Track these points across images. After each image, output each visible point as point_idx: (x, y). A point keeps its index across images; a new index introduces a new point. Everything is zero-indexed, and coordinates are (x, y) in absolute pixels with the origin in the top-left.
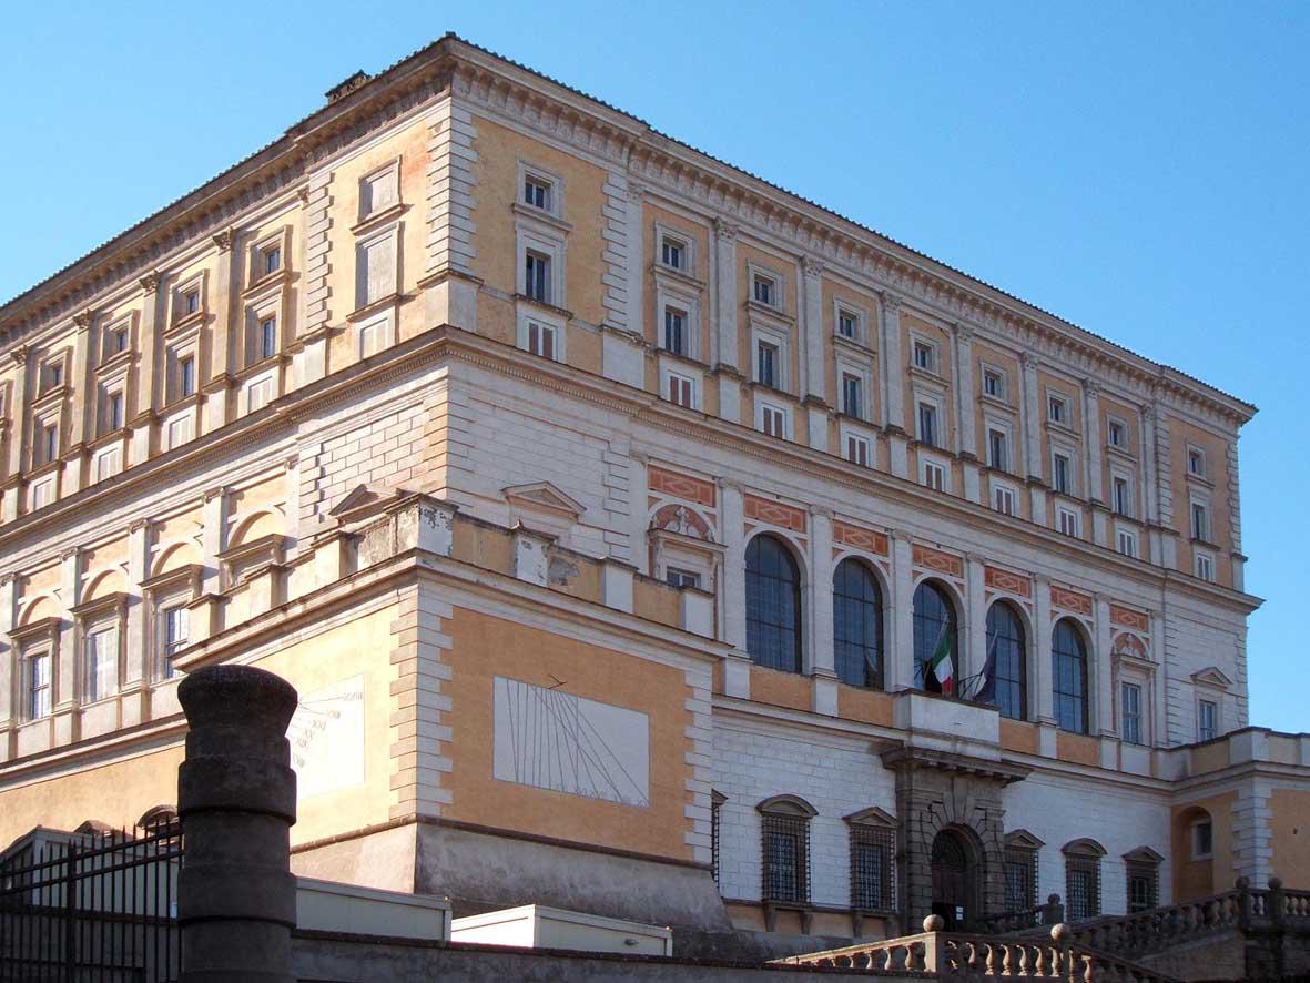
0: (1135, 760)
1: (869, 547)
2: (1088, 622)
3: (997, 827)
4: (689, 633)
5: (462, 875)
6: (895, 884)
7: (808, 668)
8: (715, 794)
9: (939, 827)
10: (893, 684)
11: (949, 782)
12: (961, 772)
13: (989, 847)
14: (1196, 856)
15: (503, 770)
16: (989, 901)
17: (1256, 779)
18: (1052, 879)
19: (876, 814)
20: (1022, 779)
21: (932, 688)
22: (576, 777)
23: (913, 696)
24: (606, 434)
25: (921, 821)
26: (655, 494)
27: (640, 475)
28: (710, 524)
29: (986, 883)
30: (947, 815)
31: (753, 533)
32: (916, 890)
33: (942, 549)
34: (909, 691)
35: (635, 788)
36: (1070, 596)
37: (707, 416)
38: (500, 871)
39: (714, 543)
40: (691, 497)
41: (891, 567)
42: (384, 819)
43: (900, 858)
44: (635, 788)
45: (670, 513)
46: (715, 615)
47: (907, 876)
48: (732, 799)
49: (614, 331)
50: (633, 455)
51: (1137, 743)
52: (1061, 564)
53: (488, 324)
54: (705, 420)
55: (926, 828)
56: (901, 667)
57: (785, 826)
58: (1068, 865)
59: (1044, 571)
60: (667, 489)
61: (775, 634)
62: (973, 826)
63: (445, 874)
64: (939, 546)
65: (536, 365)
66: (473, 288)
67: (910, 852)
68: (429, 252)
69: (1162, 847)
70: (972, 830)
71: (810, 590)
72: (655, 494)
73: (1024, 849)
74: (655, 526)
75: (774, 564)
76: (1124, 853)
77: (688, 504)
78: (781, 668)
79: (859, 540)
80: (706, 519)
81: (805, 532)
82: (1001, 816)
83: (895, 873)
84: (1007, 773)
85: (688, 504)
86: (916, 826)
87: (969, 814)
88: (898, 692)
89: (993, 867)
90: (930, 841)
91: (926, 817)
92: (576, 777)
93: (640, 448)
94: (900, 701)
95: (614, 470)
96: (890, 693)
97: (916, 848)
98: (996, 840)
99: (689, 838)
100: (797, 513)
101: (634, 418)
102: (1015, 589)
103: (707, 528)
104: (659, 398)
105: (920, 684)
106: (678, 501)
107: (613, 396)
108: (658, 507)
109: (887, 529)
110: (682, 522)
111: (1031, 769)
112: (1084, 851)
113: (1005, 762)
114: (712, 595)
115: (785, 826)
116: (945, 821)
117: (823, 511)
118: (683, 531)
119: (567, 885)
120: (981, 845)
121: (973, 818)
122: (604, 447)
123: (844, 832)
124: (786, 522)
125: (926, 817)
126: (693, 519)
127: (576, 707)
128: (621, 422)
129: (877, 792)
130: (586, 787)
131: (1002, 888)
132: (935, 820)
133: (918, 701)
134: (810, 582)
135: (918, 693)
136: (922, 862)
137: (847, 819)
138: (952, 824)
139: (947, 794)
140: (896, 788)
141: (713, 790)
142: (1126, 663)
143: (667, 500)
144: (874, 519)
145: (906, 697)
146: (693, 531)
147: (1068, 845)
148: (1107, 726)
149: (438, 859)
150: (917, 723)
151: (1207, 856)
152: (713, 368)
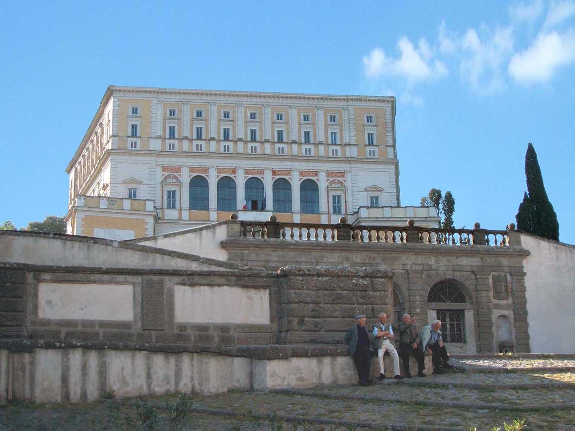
2: (316, 179)
27: (159, 170)
40: (174, 172)
49: (152, 138)
50: (157, 165)
61: (199, 200)
65: (133, 151)
77: (171, 173)
79: (226, 172)
85: (173, 173)
93: (158, 163)
103: (178, 178)
106: (170, 173)
126: (175, 177)
128: (154, 159)
144: (231, 165)
146: (175, 180)
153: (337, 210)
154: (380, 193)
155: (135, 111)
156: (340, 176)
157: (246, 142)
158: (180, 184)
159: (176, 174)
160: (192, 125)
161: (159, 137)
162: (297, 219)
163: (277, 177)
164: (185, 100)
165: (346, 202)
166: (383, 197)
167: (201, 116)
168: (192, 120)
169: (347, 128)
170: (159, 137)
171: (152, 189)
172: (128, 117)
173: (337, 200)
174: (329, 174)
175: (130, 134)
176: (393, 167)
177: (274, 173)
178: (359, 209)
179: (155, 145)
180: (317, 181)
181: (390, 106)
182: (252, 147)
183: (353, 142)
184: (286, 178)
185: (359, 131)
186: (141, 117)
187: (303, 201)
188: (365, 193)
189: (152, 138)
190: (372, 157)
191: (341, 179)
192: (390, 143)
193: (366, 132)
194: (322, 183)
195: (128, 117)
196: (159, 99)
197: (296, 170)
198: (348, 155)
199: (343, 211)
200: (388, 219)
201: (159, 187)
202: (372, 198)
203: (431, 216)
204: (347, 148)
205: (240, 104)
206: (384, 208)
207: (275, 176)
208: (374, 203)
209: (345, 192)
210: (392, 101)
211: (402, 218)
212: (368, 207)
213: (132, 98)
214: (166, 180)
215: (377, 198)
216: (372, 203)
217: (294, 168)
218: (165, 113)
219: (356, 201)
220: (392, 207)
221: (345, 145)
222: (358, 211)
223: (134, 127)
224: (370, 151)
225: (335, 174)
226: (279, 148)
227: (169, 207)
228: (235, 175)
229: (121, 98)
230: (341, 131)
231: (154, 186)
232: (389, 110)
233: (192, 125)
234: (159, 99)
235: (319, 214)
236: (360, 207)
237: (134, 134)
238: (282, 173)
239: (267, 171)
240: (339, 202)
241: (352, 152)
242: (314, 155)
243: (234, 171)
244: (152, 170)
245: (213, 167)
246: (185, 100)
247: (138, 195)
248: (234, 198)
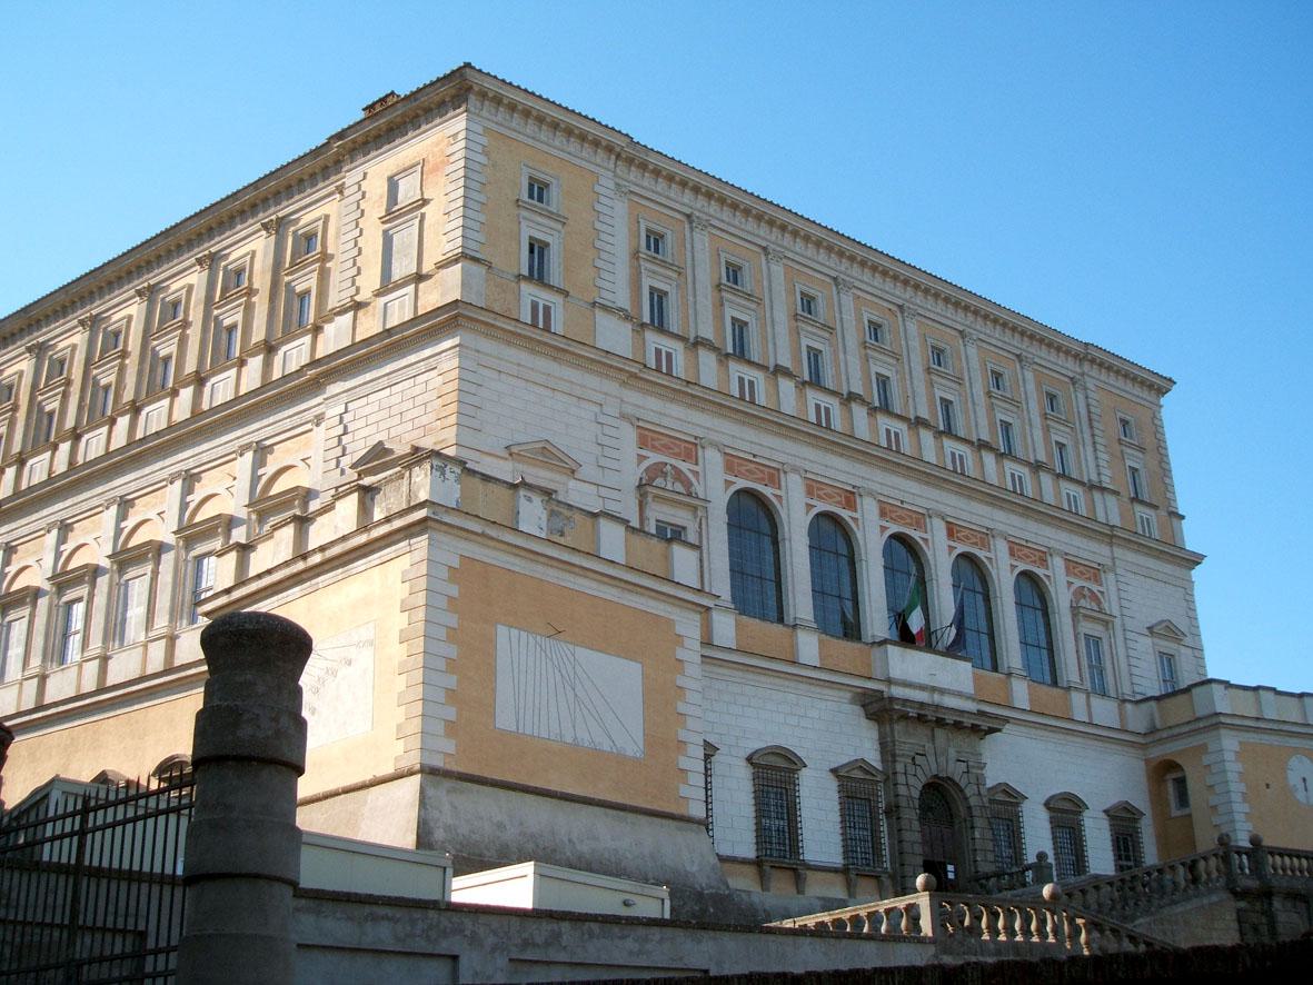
1: (838, 502)
3: (980, 781)
4: (678, 583)
5: (464, 830)
6: (885, 840)
7: (789, 619)
8: (707, 744)
9: (924, 780)
10: (870, 634)
11: (929, 733)
12: (940, 722)
13: (973, 801)
14: (1175, 813)
15: (505, 720)
16: (978, 859)
17: (1223, 732)
18: (1038, 837)
19: (861, 765)
20: (999, 730)
21: (906, 638)
22: (574, 727)
23: (889, 646)
24: (598, 397)
25: (905, 774)
26: (643, 452)
27: (629, 435)
28: (693, 480)
29: (973, 839)
30: (930, 767)
31: (733, 489)
32: (906, 846)
33: (905, 506)
34: (884, 642)
35: (631, 741)
37: (688, 382)
38: (500, 826)
39: (697, 498)
40: (677, 455)
41: (860, 522)
42: (389, 770)
43: (888, 812)
44: (631, 741)
45: (657, 470)
46: (702, 567)
47: (897, 833)
48: (723, 749)
49: (604, 308)
50: (623, 416)
51: (1104, 694)
52: (1015, 520)
53: (495, 300)
54: (687, 386)
55: (912, 781)
56: (877, 621)
57: (775, 777)
59: (1001, 527)
60: (654, 448)
61: (758, 587)
62: (957, 779)
63: (448, 828)
64: (902, 502)
66: (482, 270)
67: (898, 807)
68: (445, 238)
69: (1141, 802)
70: (957, 785)
71: (787, 543)
72: (643, 452)
73: (1007, 803)
74: (644, 482)
75: (753, 518)
76: (1105, 808)
77: (673, 462)
78: (764, 618)
79: (830, 497)
80: (690, 476)
81: (779, 488)
82: (982, 769)
83: (884, 828)
84: (985, 725)
85: (673, 462)
86: (901, 779)
87: (951, 768)
88: (874, 643)
89: (979, 822)
90: (916, 794)
91: (911, 769)
92: (574, 727)
93: (629, 410)
94: (877, 652)
95: (607, 430)
96: (867, 644)
97: (903, 803)
98: (979, 794)
99: (685, 791)
100: (772, 471)
102: (976, 544)
103: (692, 484)
104: (645, 366)
105: (895, 635)
107: (604, 363)
108: (646, 464)
109: (854, 487)
110: (669, 478)
111: (1006, 720)
112: (1067, 806)
113: (981, 713)
114: (698, 547)
115: (775, 777)
116: (929, 775)
117: (795, 470)
118: (669, 487)
119: (565, 839)
120: (966, 799)
121: (956, 771)
122: (596, 409)
123: (832, 785)
124: (763, 479)
125: (911, 769)
127: (573, 655)
128: (611, 387)
129: (862, 744)
131: (990, 846)
133: (894, 652)
134: (787, 536)
135: (894, 643)
136: (910, 815)
137: (834, 771)
138: (936, 776)
139: (928, 746)
140: (880, 739)
141: (705, 741)
142: (1085, 616)
143: (654, 458)
144: (842, 477)
145: (882, 648)
146: (679, 487)
147: (1053, 797)
148: (1074, 677)
149: (440, 812)
150: (895, 673)
151: (1186, 811)
152: (692, 340)
155: (538, 190)
188: (1149, 641)
189: (604, 308)
213: (530, 142)
223: (537, 249)
229: (495, 127)
237: (537, 274)
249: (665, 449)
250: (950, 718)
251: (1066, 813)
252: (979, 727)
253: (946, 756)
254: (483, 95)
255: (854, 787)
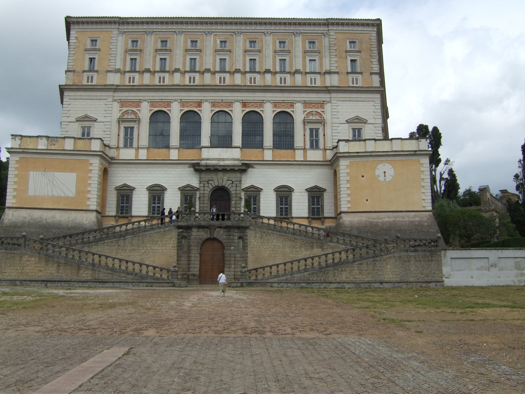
0: (315, 155)
17: (341, 159)
24: (105, 98)
27: (116, 106)
36: (283, 104)
50: (114, 101)
58: (277, 194)
61: (159, 138)
85: (131, 109)
93: (116, 98)
99: (88, 203)
101: (114, 92)
118: (129, 117)
126: (134, 112)
128: (111, 94)
130: (55, 194)
132: (210, 186)
153: (314, 145)
154: (363, 125)
156: (318, 107)
157: (214, 73)
158: (138, 120)
159: (135, 109)
160: (155, 57)
161: (118, 71)
162: (268, 155)
163: (248, 110)
164: (149, 30)
165: (324, 135)
166: (366, 128)
167: (166, 46)
168: (157, 51)
169: (327, 54)
170: (118, 71)
171: (107, 126)
172: (86, 50)
173: (314, 135)
174: (306, 104)
175: (87, 68)
176: (378, 96)
177: (244, 104)
178: (337, 143)
179: (114, 79)
180: (292, 113)
181: (375, 29)
182: (220, 78)
183: (333, 69)
184: (258, 110)
185: (340, 57)
186: (99, 50)
187: (245, 135)
188: (347, 125)
189: (110, 71)
190: (355, 85)
191: (319, 110)
192: (376, 69)
193: (349, 59)
194: (299, 114)
195: (86, 50)
196: (121, 30)
197: (269, 101)
198: (328, 84)
199: (321, 146)
200: (372, 154)
201: (115, 125)
202: (354, 130)
203: (421, 149)
204: (327, 76)
205: (209, 32)
206: (367, 141)
207: (245, 109)
208: (357, 136)
209: (324, 125)
210: (377, 24)
211: (387, 152)
212: (347, 141)
214: (124, 116)
215: (360, 130)
216: (354, 135)
217: (267, 99)
218: (126, 44)
219: (337, 134)
220: (376, 140)
221: (325, 73)
222: (337, 146)
224: (353, 79)
225: (313, 104)
226: (251, 78)
227: (126, 146)
228: (200, 109)
230: (321, 59)
231: (110, 123)
232: (374, 34)
233: (155, 57)
234: (121, 30)
235: (294, 149)
236: (339, 141)
238: (253, 105)
239: (236, 103)
240: (317, 136)
241: (333, 81)
242: (289, 85)
243: (199, 104)
244: (108, 106)
245: (176, 100)
246: (149, 30)
247: (91, 133)
248: (198, 135)
249: (130, 106)
250: (212, 168)
251: (284, 195)
252: (244, 168)
253: (223, 180)
254: (74, 23)
255: (187, 194)
